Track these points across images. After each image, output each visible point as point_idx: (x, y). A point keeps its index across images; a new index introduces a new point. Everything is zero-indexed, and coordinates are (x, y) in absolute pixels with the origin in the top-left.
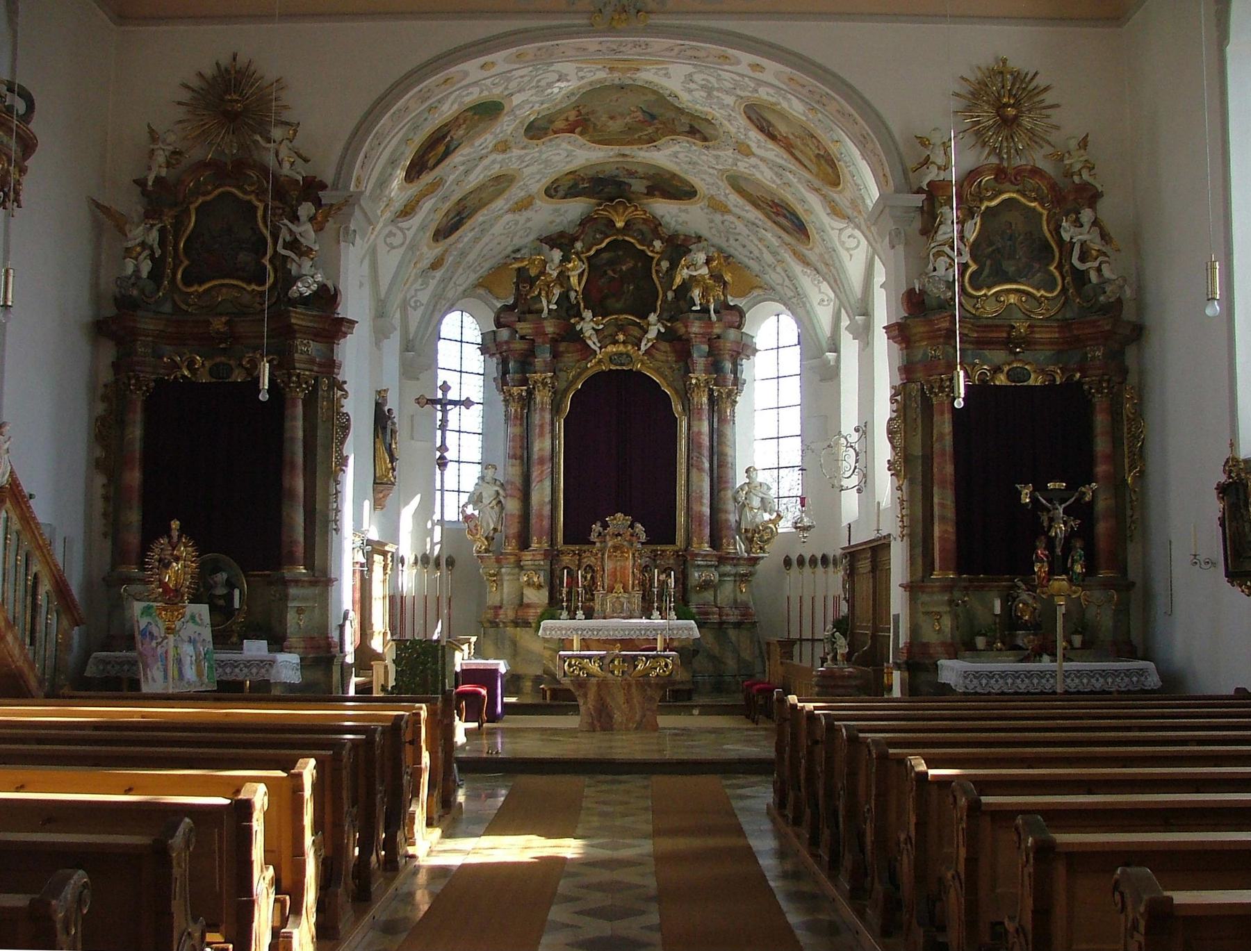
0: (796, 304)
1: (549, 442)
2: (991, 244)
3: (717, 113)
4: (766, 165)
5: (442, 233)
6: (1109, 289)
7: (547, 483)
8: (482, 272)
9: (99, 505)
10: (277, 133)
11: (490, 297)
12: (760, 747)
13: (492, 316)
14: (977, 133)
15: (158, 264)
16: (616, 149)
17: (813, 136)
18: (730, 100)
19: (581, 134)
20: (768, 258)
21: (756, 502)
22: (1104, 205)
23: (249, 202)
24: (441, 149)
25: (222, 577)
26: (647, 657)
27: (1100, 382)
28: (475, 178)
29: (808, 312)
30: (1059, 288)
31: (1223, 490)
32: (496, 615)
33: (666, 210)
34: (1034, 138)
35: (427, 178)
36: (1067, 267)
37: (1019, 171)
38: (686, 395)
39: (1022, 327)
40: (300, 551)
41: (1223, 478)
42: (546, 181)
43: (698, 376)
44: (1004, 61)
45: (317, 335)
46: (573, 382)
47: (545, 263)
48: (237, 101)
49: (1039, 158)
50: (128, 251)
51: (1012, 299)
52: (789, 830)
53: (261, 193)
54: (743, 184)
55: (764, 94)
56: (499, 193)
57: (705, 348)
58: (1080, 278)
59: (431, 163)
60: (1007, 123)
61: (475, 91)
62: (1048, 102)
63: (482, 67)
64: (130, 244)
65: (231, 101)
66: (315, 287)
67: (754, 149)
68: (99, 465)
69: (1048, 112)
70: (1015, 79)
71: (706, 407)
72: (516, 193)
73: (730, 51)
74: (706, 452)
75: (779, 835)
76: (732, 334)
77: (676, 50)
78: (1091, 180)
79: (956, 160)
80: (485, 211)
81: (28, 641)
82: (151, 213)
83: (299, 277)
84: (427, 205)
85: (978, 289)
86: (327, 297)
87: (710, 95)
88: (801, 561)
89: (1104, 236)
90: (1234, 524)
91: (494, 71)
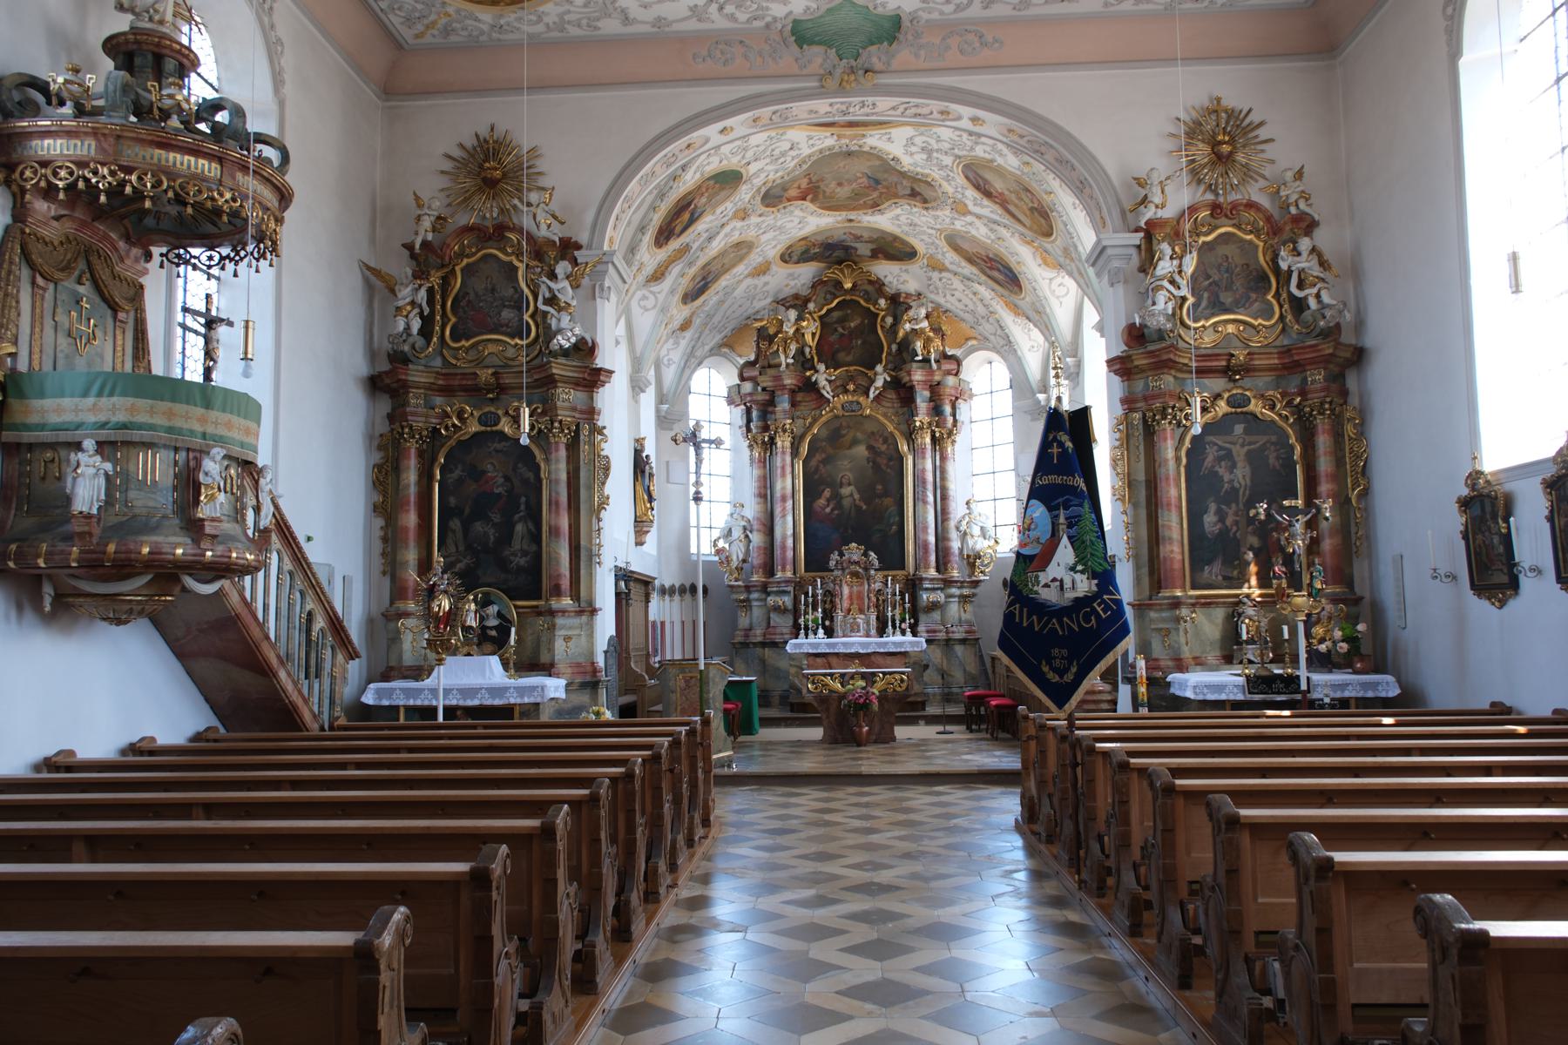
0: (1007, 349)
1: (791, 480)
2: (1208, 277)
3: (936, 174)
4: (983, 224)
5: (691, 296)
6: (1328, 313)
7: (790, 518)
8: (727, 331)
9: (378, 546)
11: (733, 355)
12: (1006, 760)
13: (735, 372)
15: (427, 322)
16: (843, 215)
17: (1028, 190)
18: (948, 160)
19: (812, 201)
20: (981, 310)
21: (976, 531)
22: (1317, 233)
24: (686, 216)
25: (492, 610)
26: (884, 674)
27: (1322, 404)
28: (717, 246)
30: (1277, 316)
31: (1465, 504)
32: (747, 636)
34: (1248, 173)
35: (674, 244)
36: (1284, 295)
37: (1235, 206)
38: (910, 435)
39: (1241, 355)
40: (565, 583)
41: (1465, 492)
42: (780, 248)
43: (922, 417)
44: (1219, 100)
45: (577, 384)
47: (781, 323)
49: (1256, 193)
50: (398, 309)
51: (1231, 329)
52: (1042, 847)
53: (519, 255)
54: (959, 242)
55: (980, 151)
56: (741, 259)
57: (927, 394)
58: (1299, 305)
59: (678, 229)
60: (1221, 160)
61: (715, 160)
62: (1262, 138)
63: (721, 132)
64: (400, 303)
66: (573, 340)
67: (971, 207)
68: (377, 509)
70: (1229, 117)
71: (929, 447)
72: (755, 259)
73: (953, 107)
74: (930, 487)
75: (1030, 850)
76: (951, 380)
77: (901, 109)
78: (1308, 210)
80: (727, 276)
81: (302, 676)
82: (420, 274)
83: (560, 331)
84: (676, 270)
85: (1195, 321)
86: (584, 349)
87: (929, 158)
89: (1323, 264)
90: (1479, 537)
91: (732, 136)
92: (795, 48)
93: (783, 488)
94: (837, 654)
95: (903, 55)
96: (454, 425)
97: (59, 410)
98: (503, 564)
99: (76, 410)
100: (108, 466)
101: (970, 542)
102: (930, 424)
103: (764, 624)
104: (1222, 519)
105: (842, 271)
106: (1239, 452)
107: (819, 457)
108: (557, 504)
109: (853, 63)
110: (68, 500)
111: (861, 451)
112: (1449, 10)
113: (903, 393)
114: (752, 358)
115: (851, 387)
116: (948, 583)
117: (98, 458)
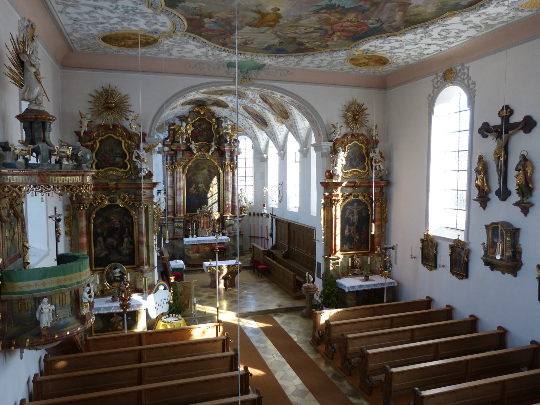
1: (182, 184)
7: (182, 196)
10: (130, 118)
14: (348, 124)
20: (248, 126)
21: (243, 199)
22: (379, 145)
23: (119, 140)
25: (118, 270)
29: (259, 142)
31: (423, 241)
33: (216, 110)
37: (358, 135)
38: (223, 166)
39: (358, 182)
41: (423, 238)
43: (227, 162)
46: (188, 163)
48: (111, 103)
51: (355, 173)
53: (121, 135)
57: (229, 153)
65: (109, 103)
69: (366, 116)
79: (342, 131)
88: (254, 214)
92: (227, 68)
93: (180, 186)
94: (201, 244)
95: (262, 74)
96: (98, 202)
97: (28, 286)
98: (120, 253)
99: (36, 285)
100: (53, 307)
101: (241, 203)
102: (230, 164)
103: (173, 232)
104: (349, 231)
105: (201, 109)
106: (355, 211)
107: (191, 173)
108: (142, 233)
109: (245, 75)
110: (38, 323)
111: (206, 171)
112: (430, 98)
113: (221, 153)
114: (166, 137)
115: (203, 149)
116: (235, 217)
117: (49, 305)
